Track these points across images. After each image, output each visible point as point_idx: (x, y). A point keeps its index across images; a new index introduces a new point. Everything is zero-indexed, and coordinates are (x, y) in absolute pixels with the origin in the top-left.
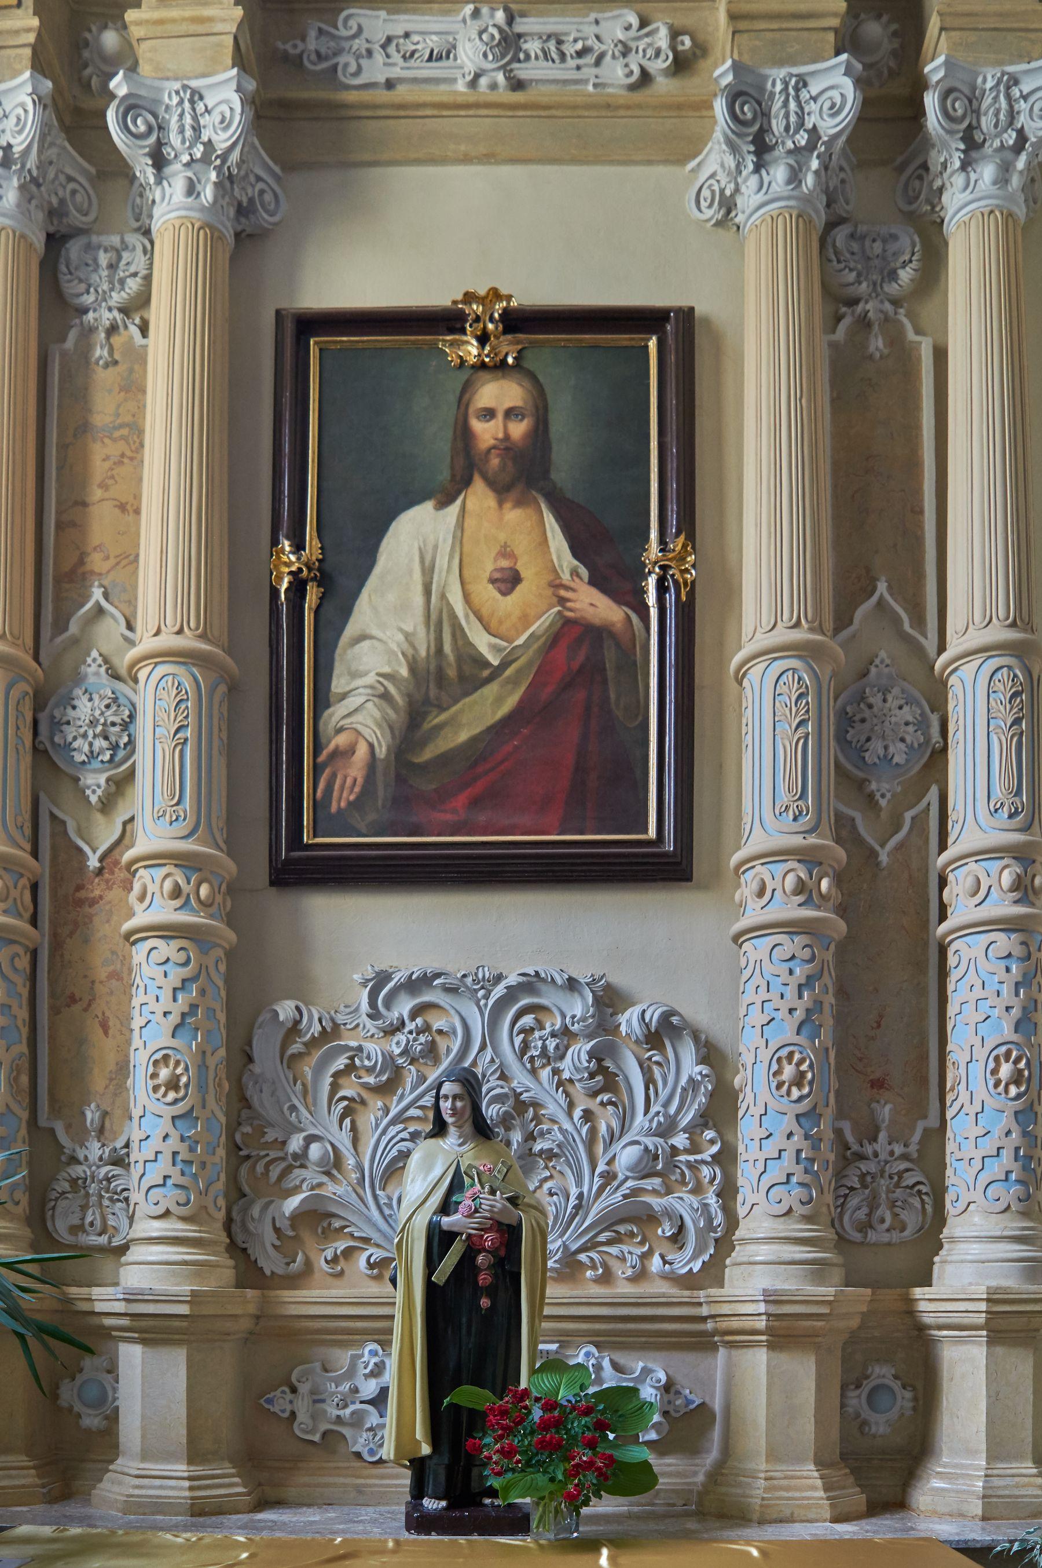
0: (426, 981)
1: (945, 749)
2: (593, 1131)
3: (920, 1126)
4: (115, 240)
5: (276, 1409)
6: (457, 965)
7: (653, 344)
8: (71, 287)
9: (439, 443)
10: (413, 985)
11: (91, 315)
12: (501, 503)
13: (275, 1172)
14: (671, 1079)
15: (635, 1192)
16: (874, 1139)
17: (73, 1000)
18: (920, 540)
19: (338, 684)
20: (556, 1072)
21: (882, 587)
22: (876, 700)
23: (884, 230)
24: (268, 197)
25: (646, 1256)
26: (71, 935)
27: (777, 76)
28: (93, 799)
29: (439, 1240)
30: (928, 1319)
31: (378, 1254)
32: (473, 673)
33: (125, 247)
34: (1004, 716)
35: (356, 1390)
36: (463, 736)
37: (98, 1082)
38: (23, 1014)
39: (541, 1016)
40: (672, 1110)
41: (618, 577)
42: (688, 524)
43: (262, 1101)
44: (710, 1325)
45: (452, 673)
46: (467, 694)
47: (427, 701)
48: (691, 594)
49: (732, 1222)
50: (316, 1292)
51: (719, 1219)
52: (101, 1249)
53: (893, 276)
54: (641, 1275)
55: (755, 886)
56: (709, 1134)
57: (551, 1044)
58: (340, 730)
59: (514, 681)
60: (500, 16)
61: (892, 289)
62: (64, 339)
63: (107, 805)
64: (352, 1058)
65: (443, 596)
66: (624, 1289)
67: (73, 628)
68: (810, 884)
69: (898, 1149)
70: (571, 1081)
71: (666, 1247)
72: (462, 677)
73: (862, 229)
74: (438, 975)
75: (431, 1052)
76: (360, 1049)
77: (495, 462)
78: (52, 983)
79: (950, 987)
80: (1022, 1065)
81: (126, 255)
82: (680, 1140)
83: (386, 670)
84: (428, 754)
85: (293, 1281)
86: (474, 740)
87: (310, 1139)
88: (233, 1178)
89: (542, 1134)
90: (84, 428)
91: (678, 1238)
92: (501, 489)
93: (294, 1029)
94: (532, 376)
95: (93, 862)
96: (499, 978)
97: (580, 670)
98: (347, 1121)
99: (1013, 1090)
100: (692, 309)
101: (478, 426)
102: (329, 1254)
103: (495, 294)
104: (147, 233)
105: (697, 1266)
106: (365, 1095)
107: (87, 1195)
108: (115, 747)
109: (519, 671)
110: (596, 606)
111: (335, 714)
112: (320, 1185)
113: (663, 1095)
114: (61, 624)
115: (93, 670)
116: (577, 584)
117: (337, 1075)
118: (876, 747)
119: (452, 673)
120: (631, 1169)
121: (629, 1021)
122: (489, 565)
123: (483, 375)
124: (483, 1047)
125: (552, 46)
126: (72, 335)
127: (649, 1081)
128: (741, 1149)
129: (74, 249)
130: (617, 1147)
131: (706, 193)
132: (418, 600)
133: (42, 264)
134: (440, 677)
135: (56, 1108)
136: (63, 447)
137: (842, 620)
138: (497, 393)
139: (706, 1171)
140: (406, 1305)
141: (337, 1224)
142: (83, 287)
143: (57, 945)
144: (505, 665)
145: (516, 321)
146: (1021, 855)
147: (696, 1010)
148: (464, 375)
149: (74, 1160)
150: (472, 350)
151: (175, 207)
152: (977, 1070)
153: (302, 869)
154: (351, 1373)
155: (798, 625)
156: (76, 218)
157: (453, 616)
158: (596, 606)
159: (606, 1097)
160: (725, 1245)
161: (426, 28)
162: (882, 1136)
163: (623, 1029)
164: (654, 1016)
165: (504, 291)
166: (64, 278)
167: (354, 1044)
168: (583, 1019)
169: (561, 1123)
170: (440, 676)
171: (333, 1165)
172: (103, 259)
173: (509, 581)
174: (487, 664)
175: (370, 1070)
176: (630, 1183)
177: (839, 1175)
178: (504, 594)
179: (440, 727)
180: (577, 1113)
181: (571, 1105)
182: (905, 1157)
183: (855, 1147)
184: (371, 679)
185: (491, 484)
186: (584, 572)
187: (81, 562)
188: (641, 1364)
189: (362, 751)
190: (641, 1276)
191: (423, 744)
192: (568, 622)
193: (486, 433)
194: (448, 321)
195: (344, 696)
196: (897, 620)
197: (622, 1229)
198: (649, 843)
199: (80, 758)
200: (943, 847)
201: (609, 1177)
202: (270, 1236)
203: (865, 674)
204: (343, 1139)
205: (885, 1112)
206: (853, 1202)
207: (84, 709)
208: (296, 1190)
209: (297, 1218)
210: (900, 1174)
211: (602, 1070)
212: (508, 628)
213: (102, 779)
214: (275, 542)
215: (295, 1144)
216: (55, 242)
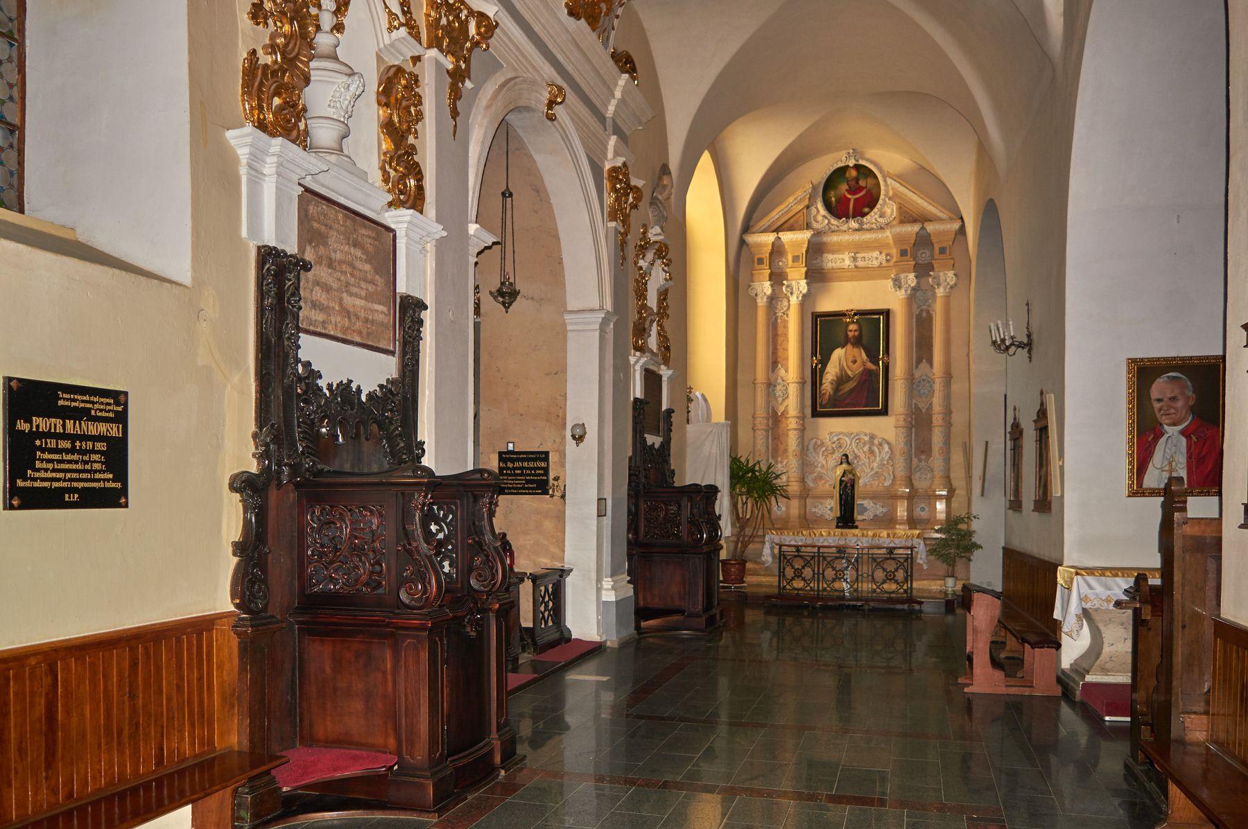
27: (902, 276)
29: (841, 481)
32: (848, 379)
92: (854, 345)
97: (868, 379)
110: (870, 366)
115: (779, 380)
121: (876, 442)
122: (851, 359)
134: (841, 380)
138: (852, 327)
153: (816, 414)
158: (870, 366)
169: (864, 460)
173: (855, 362)
193: (851, 334)
212: (854, 370)
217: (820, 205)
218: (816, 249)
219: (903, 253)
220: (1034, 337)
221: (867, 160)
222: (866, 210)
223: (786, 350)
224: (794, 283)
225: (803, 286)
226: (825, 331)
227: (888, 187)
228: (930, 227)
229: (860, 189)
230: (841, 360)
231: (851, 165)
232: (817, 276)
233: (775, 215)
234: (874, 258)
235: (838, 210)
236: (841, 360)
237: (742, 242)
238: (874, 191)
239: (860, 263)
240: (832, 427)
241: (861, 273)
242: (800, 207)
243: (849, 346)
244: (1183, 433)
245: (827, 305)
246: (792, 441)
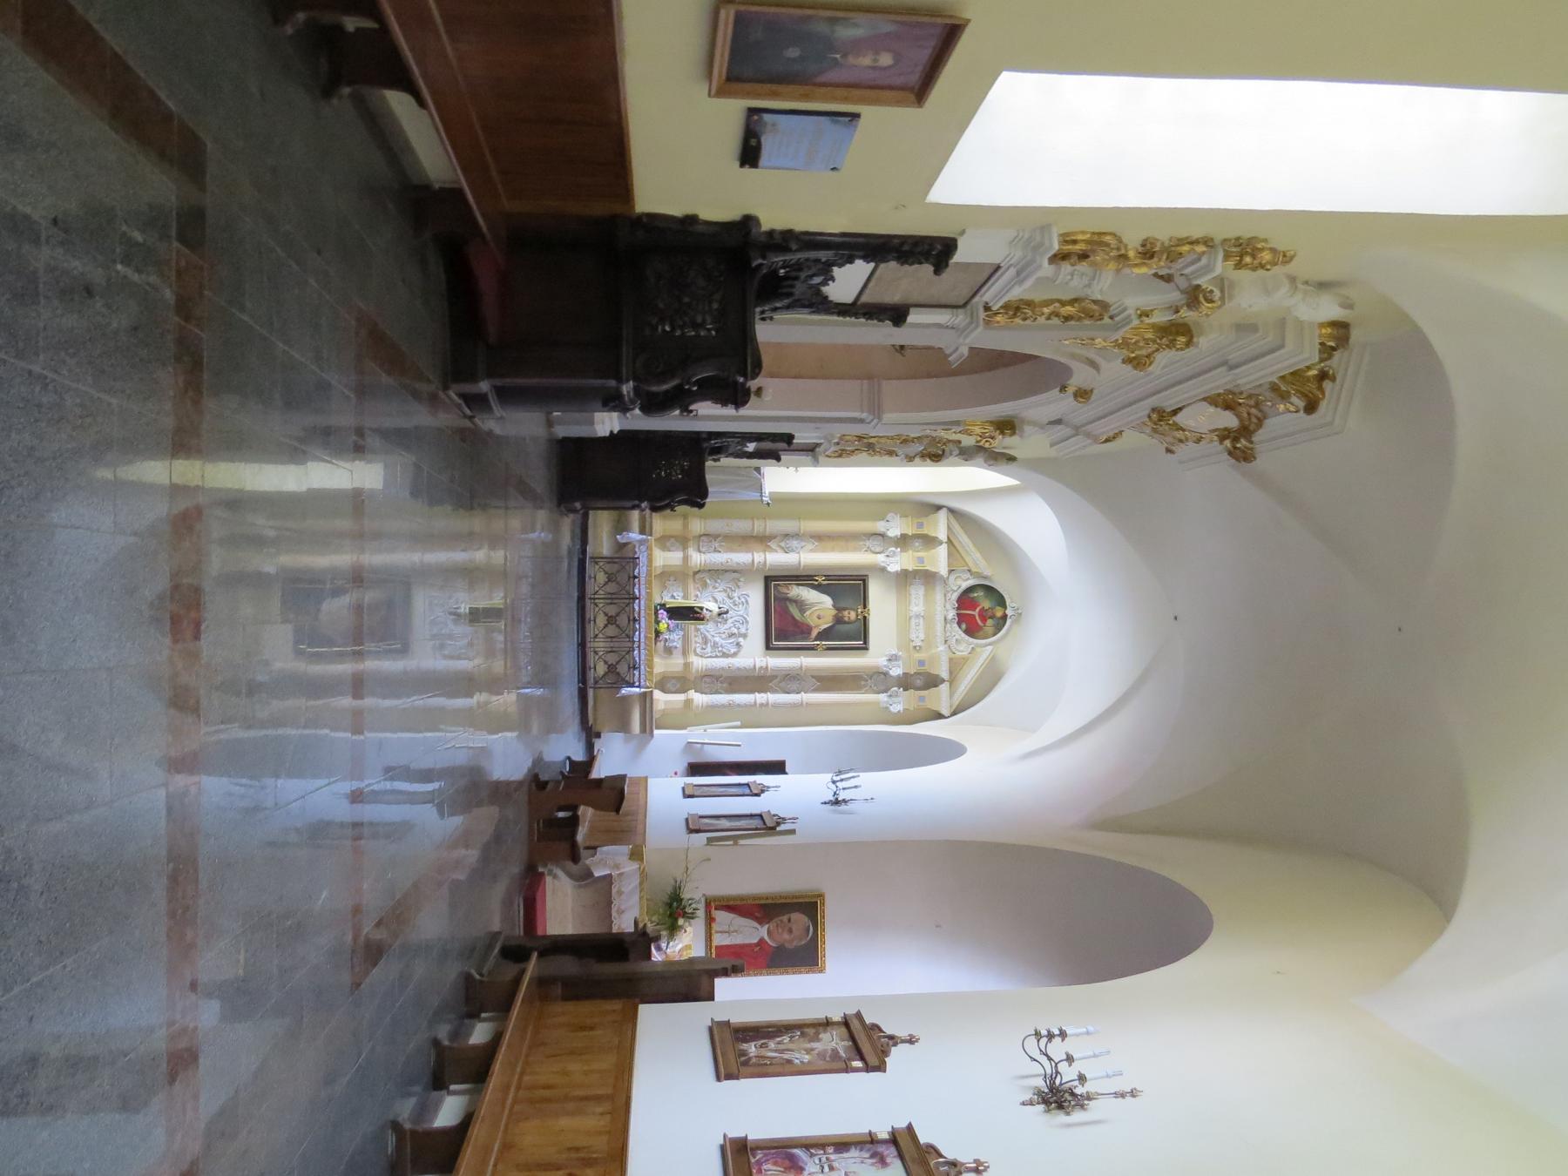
9: (842, 605)
32: (802, 611)
42: (829, 649)
97: (802, 630)
110: (814, 633)
114: (812, 537)
134: (801, 605)
138: (853, 615)
140: (690, 603)
151: (880, 559)
158: (814, 633)
169: (723, 628)
190: (696, 642)
212: (810, 618)
217: (971, 582)
218: (928, 578)
219: (921, 663)
220: (843, 807)
223: (833, 550)
225: (894, 567)
227: (983, 650)
228: (944, 687)
230: (819, 606)
232: (905, 579)
233: (963, 538)
235: (965, 600)
236: (819, 606)
237: (939, 508)
239: (913, 621)
240: (754, 598)
241: (904, 621)
242: (971, 564)
244: (762, 941)
245: (875, 590)
246: (740, 558)
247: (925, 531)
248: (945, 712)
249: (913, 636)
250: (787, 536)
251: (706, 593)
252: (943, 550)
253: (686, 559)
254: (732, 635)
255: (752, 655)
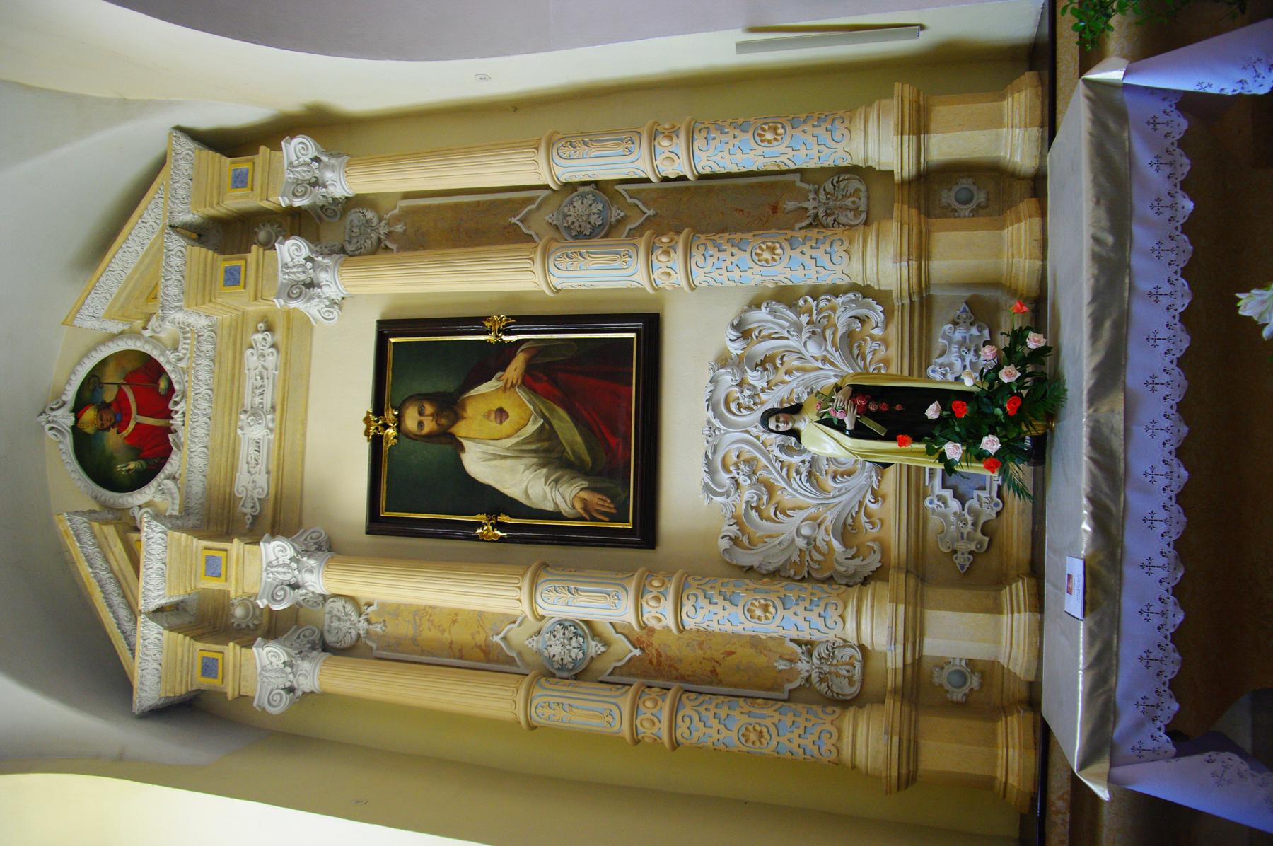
0: (709, 463)
1: (596, 183)
2: (798, 369)
3: (799, 184)
4: (327, 616)
5: (967, 564)
6: (702, 447)
7: (393, 340)
8: (348, 641)
10: (711, 471)
11: (362, 632)
12: (463, 418)
13: (817, 556)
14: (768, 325)
15: (833, 344)
16: (806, 209)
17: (714, 672)
18: (492, 202)
19: (549, 507)
20: (763, 390)
21: (514, 220)
22: (570, 219)
23: (348, 227)
24: (314, 535)
25: (873, 338)
26: (677, 669)
28: (603, 649)
30: (914, 171)
31: (869, 497)
32: (547, 434)
33: (330, 612)
34: (582, 150)
35: (955, 514)
36: (579, 439)
37: (761, 660)
38: (721, 698)
39: (731, 399)
40: (787, 324)
41: (503, 355)
42: (479, 320)
43: (776, 562)
44: (916, 298)
45: (546, 444)
46: (557, 437)
47: (560, 458)
48: (512, 317)
49: (854, 288)
50: (893, 535)
51: (851, 296)
52: (864, 667)
53: (368, 221)
54: (885, 342)
55: (665, 278)
56: (801, 303)
57: (747, 393)
58: (573, 506)
59: (551, 411)
60: (243, 416)
61: (375, 222)
62: (371, 648)
63: (606, 643)
64: (752, 508)
65: (508, 449)
66: (893, 352)
67: (513, 654)
68: (665, 247)
69: (812, 196)
70: (768, 382)
71: (867, 327)
72: (548, 440)
73: (347, 238)
74: (706, 456)
75: (750, 462)
76: (747, 502)
77: (443, 421)
78: (703, 682)
79: (722, 171)
80: (766, 127)
81: (335, 612)
82: (804, 319)
83: (543, 480)
84: (587, 458)
85: (884, 550)
86: (581, 434)
87: (798, 533)
88: (823, 581)
89: (798, 398)
90: (414, 640)
91: (863, 320)
92: (457, 418)
93: (735, 541)
94: (404, 402)
95: (637, 652)
96: (709, 422)
98: (789, 512)
99: (781, 131)
100: (379, 322)
101: (426, 430)
102: (869, 526)
103: (367, 420)
104: (325, 598)
105: (879, 308)
106: (774, 501)
107: (830, 673)
108: (576, 634)
109: (547, 409)
111: (564, 508)
112: (826, 530)
113: (777, 329)
114: (511, 661)
115: (535, 644)
116: (504, 378)
117: (761, 517)
118: (593, 219)
119: (546, 444)
120: (821, 347)
121: (735, 349)
122: (493, 424)
123: (403, 427)
124: (748, 432)
125: (258, 391)
126: (370, 643)
127: (770, 337)
128: (810, 282)
129: (330, 639)
130: (807, 355)
131: (327, 315)
132: (508, 462)
133: (335, 654)
134: (548, 452)
135: (776, 687)
136: (423, 652)
137: (529, 239)
139: (823, 304)
141: (850, 521)
142: (348, 636)
143: (682, 678)
144: (544, 417)
145: (378, 409)
146: (653, 136)
147: (730, 312)
148: (402, 437)
149: (808, 679)
150: (391, 432)
151: (319, 580)
152: (768, 151)
153: (645, 531)
154: (944, 516)
155: (532, 260)
156: (316, 637)
157: (518, 444)
159: (778, 362)
160: (865, 291)
161: (246, 452)
162: (805, 205)
163: (740, 352)
164: (733, 334)
165: (365, 415)
166: (344, 645)
167: (744, 506)
168: (733, 375)
170: (546, 451)
171: (816, 522)
172: (336, 624)
173: (501, 414)
174: (542, 428)
175: (759, 499)
176: (829, 348)
177: (826, 227)
178: (508, 416)
179: (574, 452)
180: (787, 378)
181: (782, 382)
182: (816, 192)
183: (810, 220)
184: (547, 489)
185: (454, 423)
186: (499, 374)
187: (480, 647)
188: (940, 340)
189: (584, 495)
191: (582, 461)
192: (523, 382)
193: (430, 425)
194: (377, 443)
195: (556, 504)
196: (530, 212)
197: (856, 352)
198: (638, 337)
199: (580, 655)
200: (647, 180)
201: (824, 360)
202: (857, 562)
203: (557, 227)
204: (799, 516)
205: (791, 205)
206: (842, 219)
207: (556, 650)
208: (828, 544)
209: (845, 543)
210: (827, 193)
211: (762, 364)
213: (593, 643)
214: (477, 539)
215: (801, 543)
216: (326, 648)
219: (233, 278)
221: (68, 382)
222: (163, 385)
223: (455, 616)
224: (268, 578)
226: (420, 501)
229: (121, 396)
230: (498, 451)
231: (71, 420)
232: (279, 516)
234: (260, 361)
235: (154, 451)
236: (498, 451)
238: (130, 366)
240: (689, 490)
243: (460, 430)
247: (202, 649)
248: (187, 147)
249: (272, 360)
250: (580, 673)
251: (843, 496)
252: (155, 589)
253: (914, 632)
254: (765, 363)
255: (702, 298)
